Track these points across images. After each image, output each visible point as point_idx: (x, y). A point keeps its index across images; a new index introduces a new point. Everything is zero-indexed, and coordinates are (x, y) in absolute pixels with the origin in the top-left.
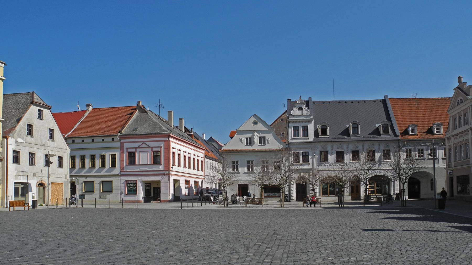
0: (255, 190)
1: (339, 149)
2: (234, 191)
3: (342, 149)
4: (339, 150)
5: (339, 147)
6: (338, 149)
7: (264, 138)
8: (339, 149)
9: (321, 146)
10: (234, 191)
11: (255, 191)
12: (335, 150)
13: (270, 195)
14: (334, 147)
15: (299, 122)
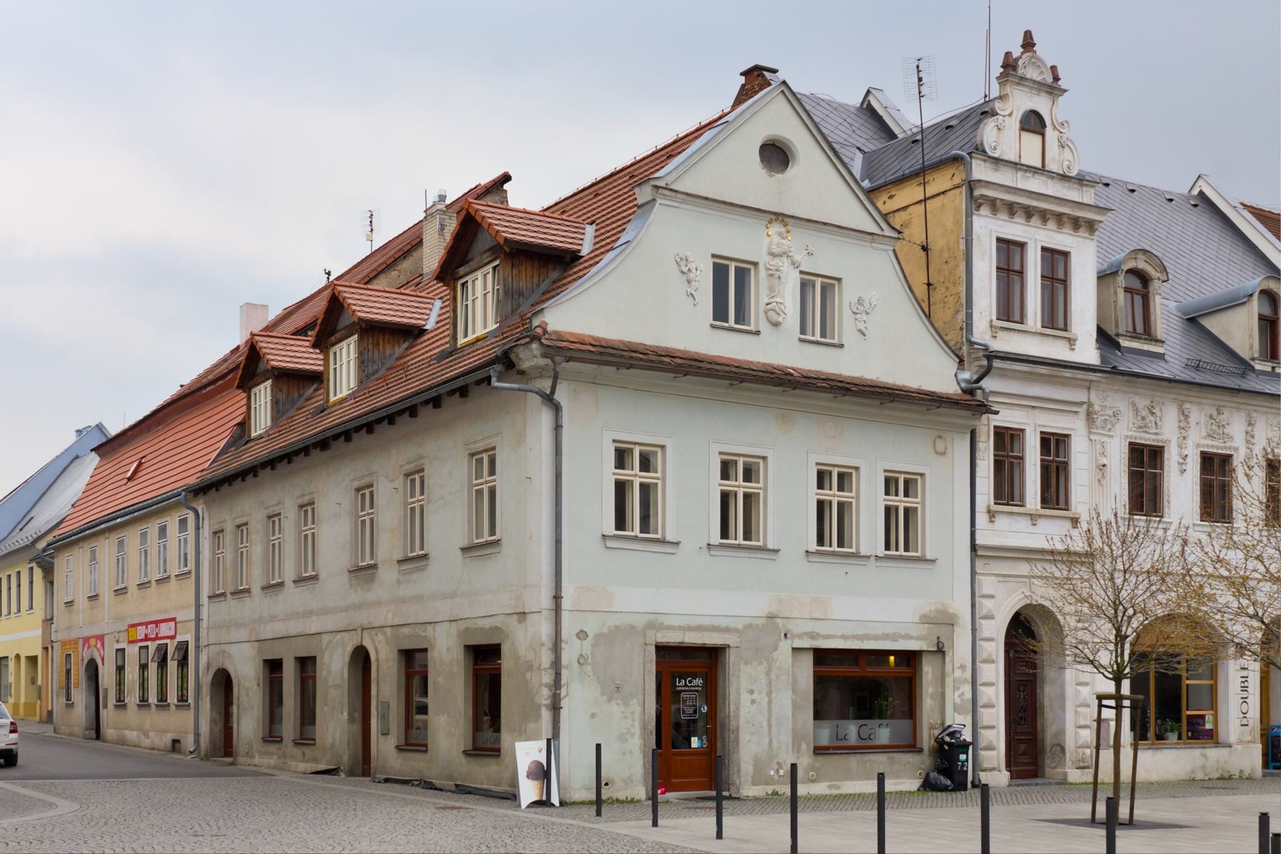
0: (769, 693)
1: (1215, 443)
2: (626, 704)
3: (1228, 444)
4: (1215, 447)
5: (1215, 427)
6: (1210, 442)
7: (830, 285)
8: (1215, 443)
9: (1134, 405)
10: (626, 704)
11: (770, 703)
12: (1198, 446)
13: (853, 739)
14: (1193, 418)
15: (1029, 213)
